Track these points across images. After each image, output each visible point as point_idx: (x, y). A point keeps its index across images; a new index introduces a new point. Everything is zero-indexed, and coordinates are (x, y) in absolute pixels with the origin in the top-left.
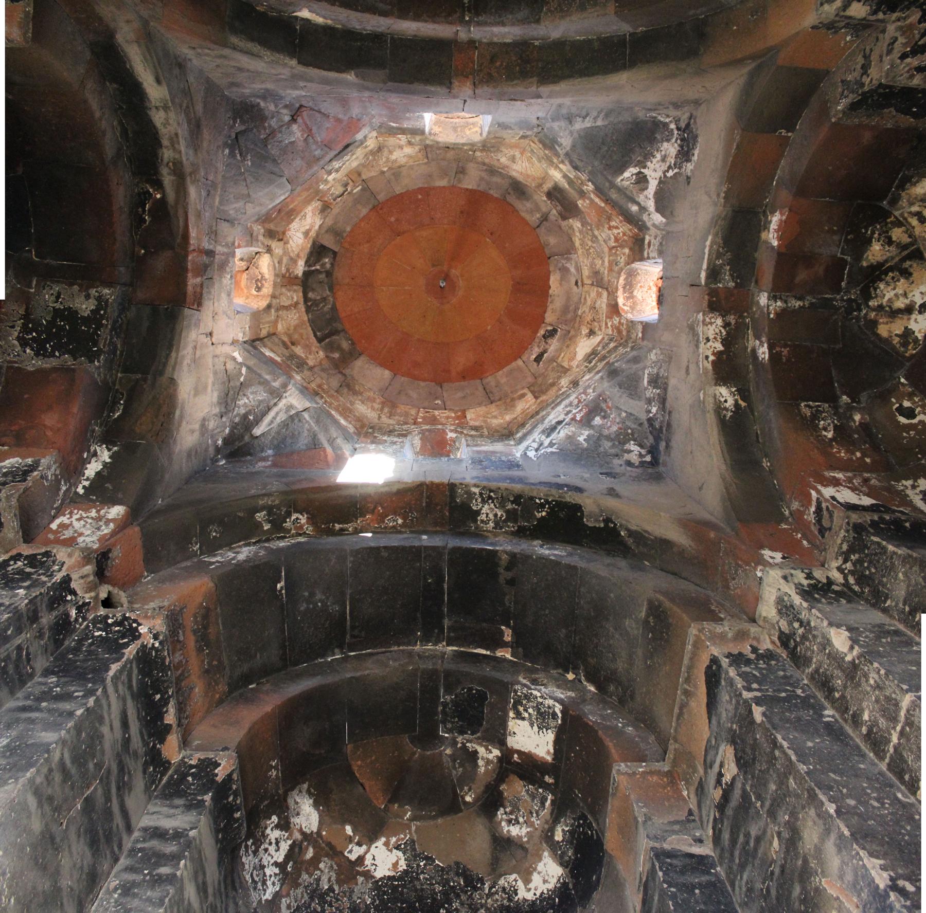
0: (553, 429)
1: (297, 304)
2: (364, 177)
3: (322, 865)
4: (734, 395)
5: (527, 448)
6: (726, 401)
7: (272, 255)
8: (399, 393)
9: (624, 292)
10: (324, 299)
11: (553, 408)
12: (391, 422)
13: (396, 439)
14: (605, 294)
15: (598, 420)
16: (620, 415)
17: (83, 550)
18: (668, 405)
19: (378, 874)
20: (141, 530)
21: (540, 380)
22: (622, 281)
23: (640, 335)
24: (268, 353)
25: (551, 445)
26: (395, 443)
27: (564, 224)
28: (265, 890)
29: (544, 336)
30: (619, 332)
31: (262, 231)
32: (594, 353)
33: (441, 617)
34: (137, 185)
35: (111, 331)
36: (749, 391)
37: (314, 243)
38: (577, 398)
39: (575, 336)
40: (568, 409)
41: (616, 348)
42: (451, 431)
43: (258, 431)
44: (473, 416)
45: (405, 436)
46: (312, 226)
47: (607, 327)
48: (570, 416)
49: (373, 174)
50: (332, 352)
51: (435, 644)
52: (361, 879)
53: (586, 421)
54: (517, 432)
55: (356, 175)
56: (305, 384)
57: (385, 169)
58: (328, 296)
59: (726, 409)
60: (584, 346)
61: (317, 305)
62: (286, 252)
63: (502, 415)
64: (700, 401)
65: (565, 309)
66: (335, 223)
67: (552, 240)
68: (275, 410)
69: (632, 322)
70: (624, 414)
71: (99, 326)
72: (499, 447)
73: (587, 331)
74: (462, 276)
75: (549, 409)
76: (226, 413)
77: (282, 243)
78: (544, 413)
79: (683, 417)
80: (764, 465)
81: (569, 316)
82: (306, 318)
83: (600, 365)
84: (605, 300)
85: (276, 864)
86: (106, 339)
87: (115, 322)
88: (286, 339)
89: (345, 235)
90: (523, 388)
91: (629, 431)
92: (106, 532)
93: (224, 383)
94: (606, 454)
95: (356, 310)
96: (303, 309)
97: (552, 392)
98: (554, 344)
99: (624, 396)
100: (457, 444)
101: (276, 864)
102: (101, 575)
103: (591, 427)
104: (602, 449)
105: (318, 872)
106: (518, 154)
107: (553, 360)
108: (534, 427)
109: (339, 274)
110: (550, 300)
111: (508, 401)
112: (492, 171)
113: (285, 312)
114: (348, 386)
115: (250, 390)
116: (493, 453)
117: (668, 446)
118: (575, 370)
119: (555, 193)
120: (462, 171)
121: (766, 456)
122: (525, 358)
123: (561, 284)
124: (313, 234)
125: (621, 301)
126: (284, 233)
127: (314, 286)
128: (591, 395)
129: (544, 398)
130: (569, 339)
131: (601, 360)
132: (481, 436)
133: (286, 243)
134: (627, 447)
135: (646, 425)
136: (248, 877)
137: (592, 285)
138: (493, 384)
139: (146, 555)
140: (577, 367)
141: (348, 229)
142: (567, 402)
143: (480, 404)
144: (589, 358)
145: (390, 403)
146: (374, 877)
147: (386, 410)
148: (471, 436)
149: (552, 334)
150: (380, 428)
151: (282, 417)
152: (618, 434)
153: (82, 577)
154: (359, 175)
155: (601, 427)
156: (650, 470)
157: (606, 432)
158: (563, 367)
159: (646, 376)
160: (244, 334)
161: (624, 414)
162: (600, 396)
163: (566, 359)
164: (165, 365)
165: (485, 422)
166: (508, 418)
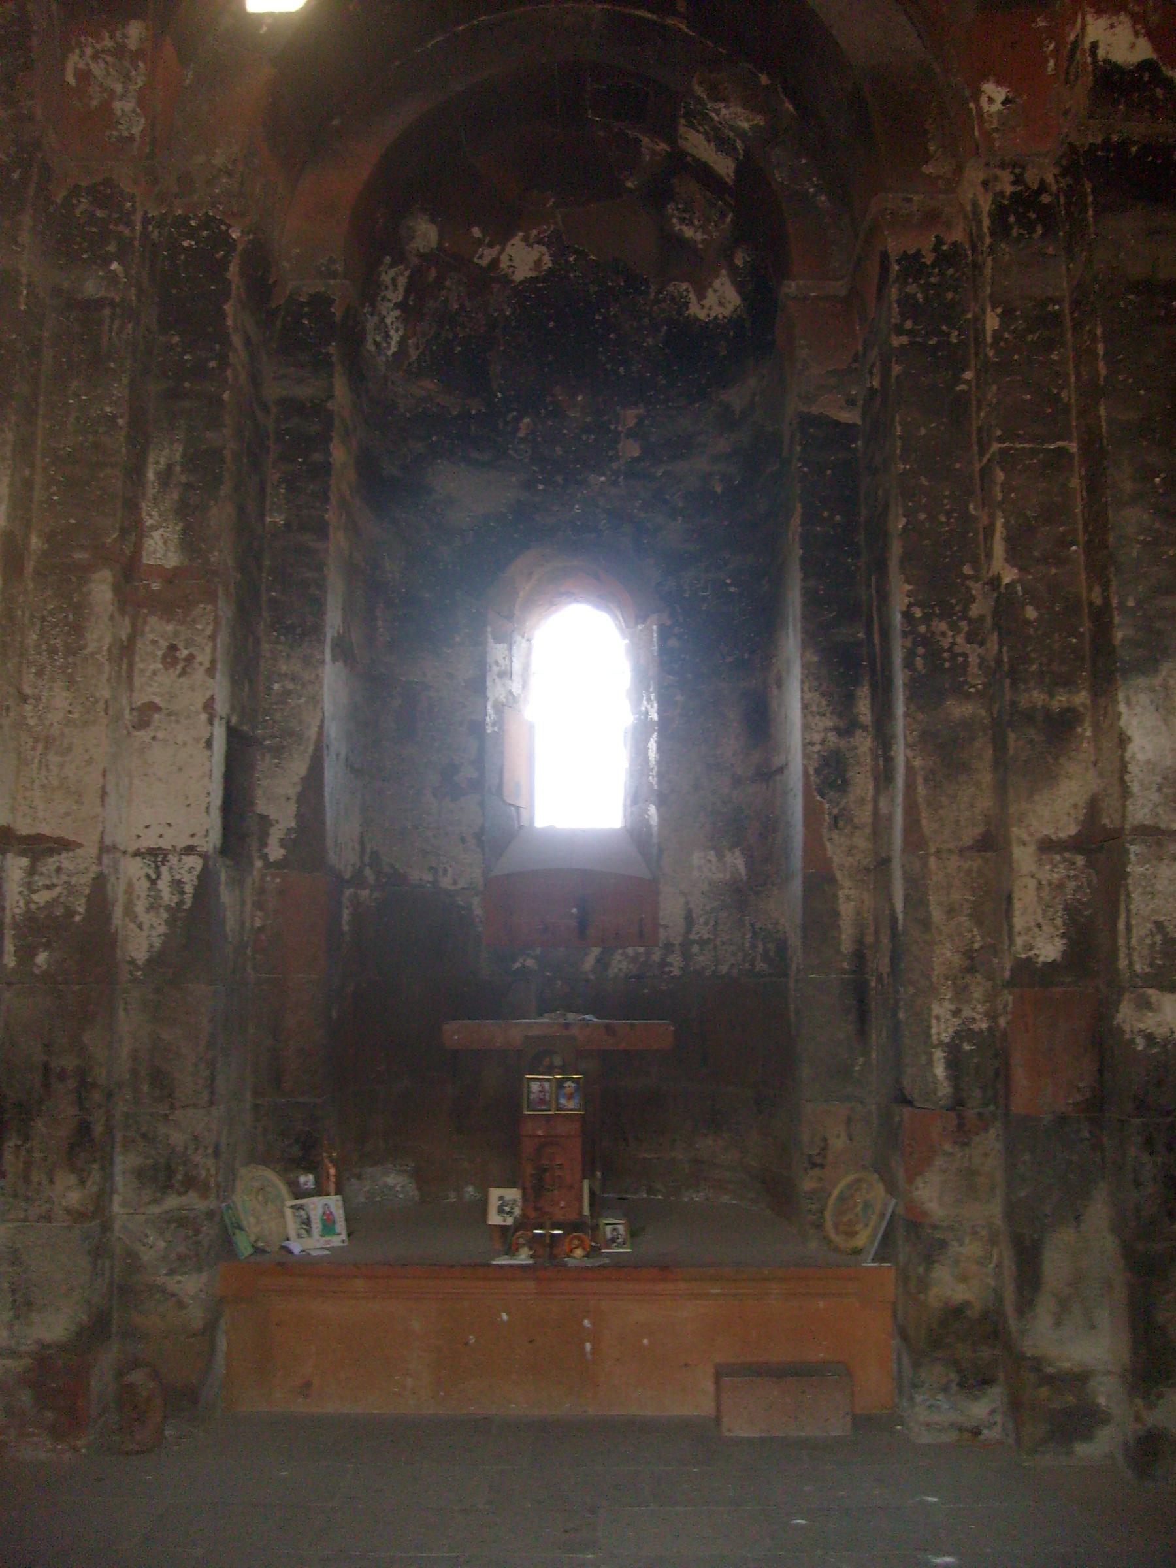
3: (448, 283)
19: (519, 276)
28: (389, 344)
52: (496, 287)
85: (397, 306)
92: (140, 83)
101: (397, 306)
105: (444, 292)
136: (372, 348)
146: (512, 281)
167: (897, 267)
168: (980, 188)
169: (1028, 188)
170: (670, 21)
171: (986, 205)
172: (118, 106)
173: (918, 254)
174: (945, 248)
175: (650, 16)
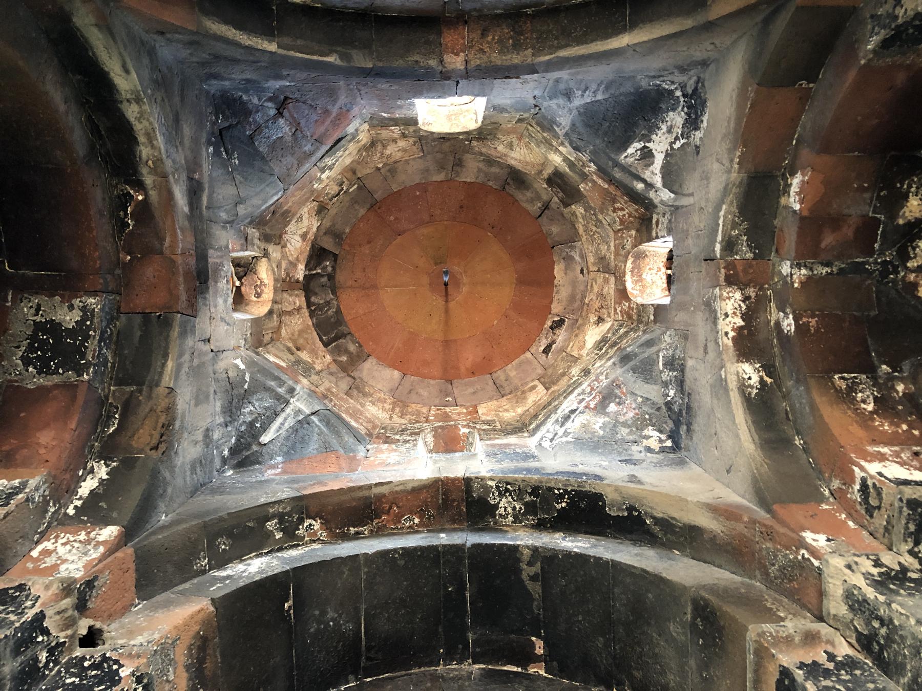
0: (567, 418)
1: (299, 309)
2: (359, 176)
4: (759, 372)
5: (542, 439)
6: (750, 378)
7: (269, 259)
8: (410, 392)
9: (633, 276)
10: (328, 303)
11: (565, 398)
12: (404, 421)
13: (408, 438)
14: (612, 279)
15: (612, 407)
16: (635, 400)
17: (62, 581)
18: (686, 388)
20: (135, 552)
21: (550, 371)
22: (629, 265)
23: (652, 318)
24: (272, 359)
25: (566, 434)
26: (408, 442)
27: (566, 211)
29: (551, 327)
30: (630, 317)
31: (257, 234)
32: (604, 340)
33: (464, 629)
34: (116, 187)
35: (100, 342)
36: (774, 366)
37: (313, 246)
38: (589, 385)
39: (583, 325)
40: (581, 397)
41: (627, 332)
42: (464, 426)
43: (265, 439)
44: (485, 411)
45: (418, 434)
46: (309, 229)
47: (616, 313)
48: (584, 404)
49: (368, 171)
50: (339, 355)
51: (460, 662)
53: (601, 408)
54: (530, 424)
55: (350, 173)
56: (313, 388)
57: (380, 165)
58: (332, 299)
59: (752, 387)
60: (593, 335)
61: (321, 310)
62: (284, 256)
63: (514, 408)
64: (722, 379)
65: (572, 298)
66: (333, 225)
67: (555, 229)
68: (283, 415)
69: (642, 305)
70: (640, 400)
71: (87, 337)
72: (512, 440)
73: (596, 318)
74: (465, 272)
75: (562, 398)
76: (230, 422)
77: (279, 247)
78: (556, 403)
79: (704, 398)
80: (797, 443)
81: (577, 304)
82: (310, 323)
83: (611, 352)
84: (613, 286)
86: (95, 351)
87: (103, 333)
88: (290, 345)
89: (344, 237)
90: (533, 381)
91: (647, 416)
92: (94, 556)
93: (227, 391)
94: (624, 442)
95: (361, 312)
96: (307, 314)
97: (564, 382)
98: (561, 335)
99: (639, 380)
100: (470, 439)
102: (81, 607)
103: (607, 414)
104: (619, 436)
106: (515, 142)
107: (562, 350)
108: (547, 417)
109: (340, 277)
110: (555, 290)
111: (518, 393)
112: (490, 161)
113: (288, 317)
114: (357, 389)
115: (255, 397)
116: (508, 445)
117: (689, 430)
118: (585, 358)
119: (556, 179)
120: (459, 164)
121: (798, 434)
122: (533, 350)
123: (566, 274)
124: (311, 236)
125: (629, 285)
126: (281, 237)
127: (317, 290)
128: (605, 382)
129: (555, 388)
130: (578, 328)
131: (612, 346)
132: (495, 430)
133: (284, 246)
134: (646, 432)
135: (664, 409)
137: (599, 271)
138: (503, 377)
139: (138, 580)
140: (588, 355)
141: (347, 230)
142: (579, 390)
143: (491, 399)
144: (599, 345)
145: (400, 403)
147: (397, 410)
148: (484, 430)
149: (559, 324)
150: (393, 428)
151: (290, 422)
152: (635, 419)
153: (59, 613)
154: (354, 173)
155: (618, 413)
156: (672, 456)
157: (622, 419)
158: (572, 356)
159: (661, 358)
160: (246, 340)
161: (640, 400)
162: (613, 382)
163: (575, 348)
164: (161, 374)
165: (497, 415)
166: (520, 410)
167: (801, 672)
168: (847, 571)
169: (892, 570)
170: (532, 670)
171: (860, 582)
172: (63, 568)
173: (814, 663)
174: (839, 659)
175: (515, 669)
